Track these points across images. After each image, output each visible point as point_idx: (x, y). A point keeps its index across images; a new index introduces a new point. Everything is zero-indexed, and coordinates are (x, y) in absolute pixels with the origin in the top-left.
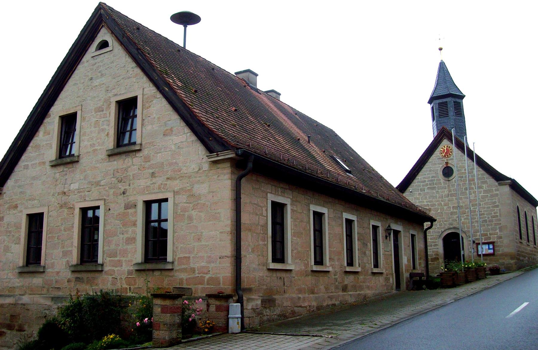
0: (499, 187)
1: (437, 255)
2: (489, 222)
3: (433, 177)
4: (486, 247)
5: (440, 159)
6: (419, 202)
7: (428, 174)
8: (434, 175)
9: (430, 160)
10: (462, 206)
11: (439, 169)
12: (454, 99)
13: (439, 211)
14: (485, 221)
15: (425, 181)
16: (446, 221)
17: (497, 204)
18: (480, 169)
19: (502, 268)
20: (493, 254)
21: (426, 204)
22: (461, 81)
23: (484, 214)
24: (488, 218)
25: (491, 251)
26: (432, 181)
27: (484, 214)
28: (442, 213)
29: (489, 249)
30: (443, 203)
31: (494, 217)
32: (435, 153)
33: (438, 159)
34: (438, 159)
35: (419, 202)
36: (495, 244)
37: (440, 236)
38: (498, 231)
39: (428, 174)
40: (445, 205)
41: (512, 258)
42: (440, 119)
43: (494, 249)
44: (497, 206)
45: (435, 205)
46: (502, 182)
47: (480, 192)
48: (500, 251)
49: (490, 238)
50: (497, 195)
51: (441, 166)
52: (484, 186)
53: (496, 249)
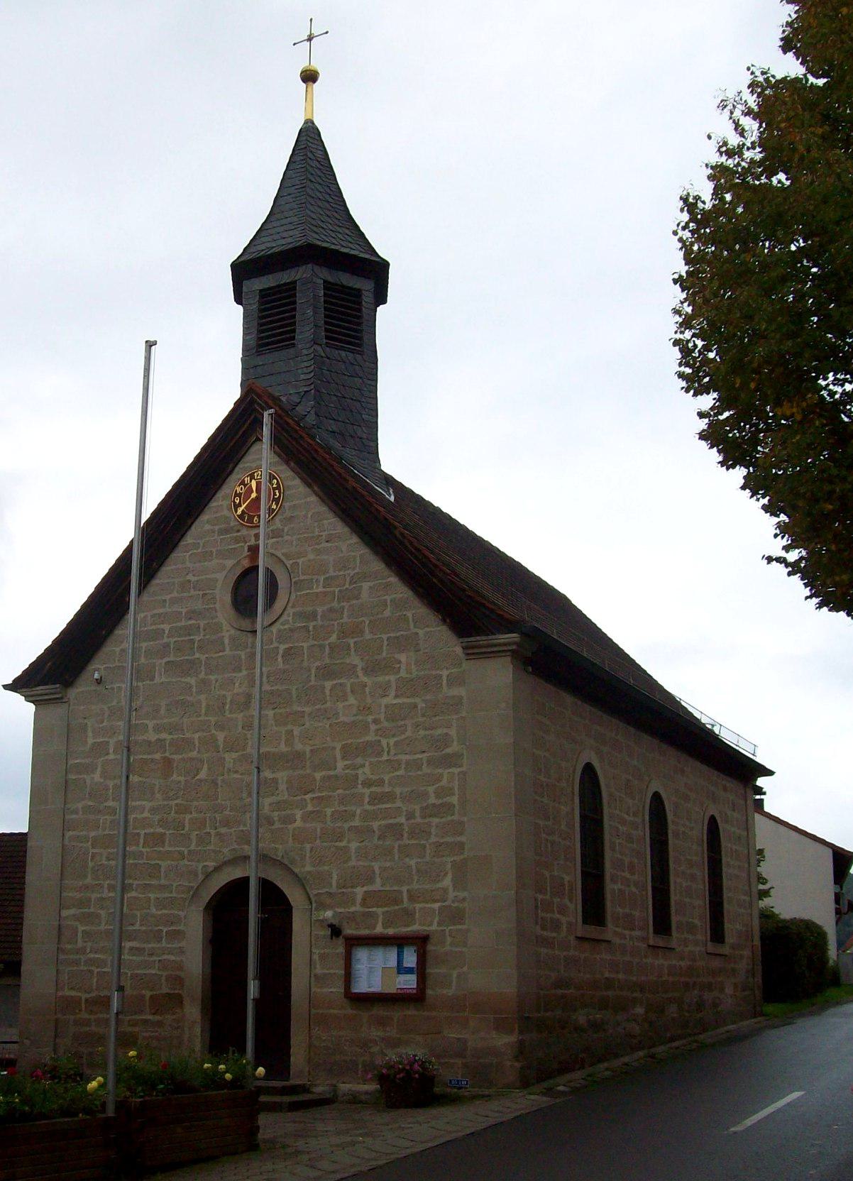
0: (466, 665)
1: (179, 981)
2: (412, 834)
3: (192, 614)
4: (388, 957)
5: (226, 531)
6: (157, 729)
7: (174, 601)
8: (199, 606)
9: (189, 539)
10: (299, 756)
11: (220, 576)
12: (325, 274)
13: (203, 774)
14: (395, 830)
15: (158, 634)
16: (226, 823)
17: (454, 748)
18: (393, 579)
19: (449, 1073)
20: (416, 998)
21: (152, 737)
22: (376, 206)
23: (389, 797)
24: (410, 816)
25: (409, 982)
26: (189, 630)
27: (389, 797)
28: (214, 783)
29: (401, 969)
30: (221, 736)
31: (429, 811)
32: (213, 504)
33: (221, 532)
34: (221, 532)
35: (157, 729)
36: (430, 947)
37: (196, 894)
38: (447, 882)
39: (174, 601)
40: (230, 748)
41: (501, 1026)
42: (259, 360)
43: (421, 971)
44: (449, 761)
45: (189, 743)
46: (482, 640)
47: (385, 689)
48: (451, 980)
49: (409, 915)
50: (459, 701)
51: (229, 563)
52: (403, 658)
53: (432, 970)
